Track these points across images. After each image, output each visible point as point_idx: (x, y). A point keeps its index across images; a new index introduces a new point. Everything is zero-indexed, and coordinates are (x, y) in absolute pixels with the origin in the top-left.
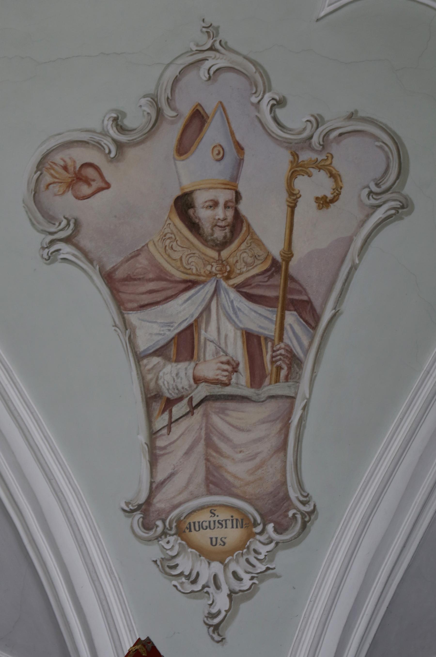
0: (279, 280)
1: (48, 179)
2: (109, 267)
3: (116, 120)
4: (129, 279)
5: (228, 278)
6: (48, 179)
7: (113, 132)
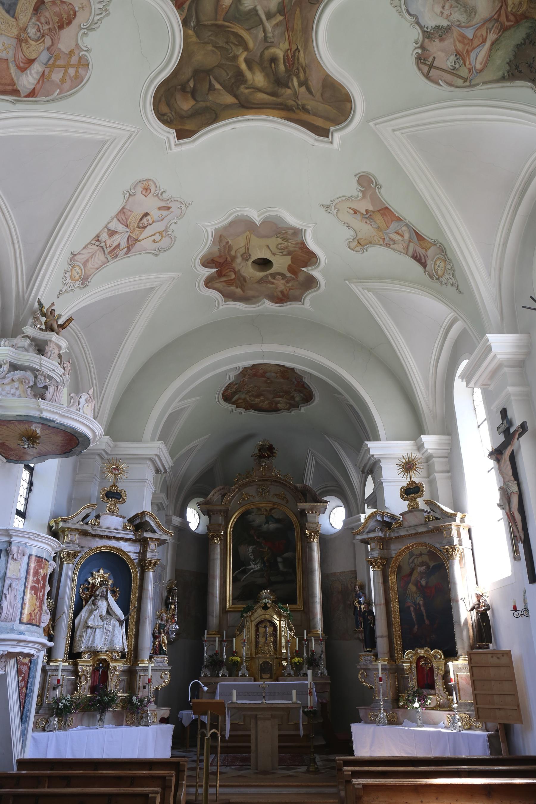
0: (134, 242)
1: (144, 183)
2: (126, 207)
3: (164, 191)
4: (124, 213)
5: (131, 232)
6: (144, 183)
7: (161, 192)
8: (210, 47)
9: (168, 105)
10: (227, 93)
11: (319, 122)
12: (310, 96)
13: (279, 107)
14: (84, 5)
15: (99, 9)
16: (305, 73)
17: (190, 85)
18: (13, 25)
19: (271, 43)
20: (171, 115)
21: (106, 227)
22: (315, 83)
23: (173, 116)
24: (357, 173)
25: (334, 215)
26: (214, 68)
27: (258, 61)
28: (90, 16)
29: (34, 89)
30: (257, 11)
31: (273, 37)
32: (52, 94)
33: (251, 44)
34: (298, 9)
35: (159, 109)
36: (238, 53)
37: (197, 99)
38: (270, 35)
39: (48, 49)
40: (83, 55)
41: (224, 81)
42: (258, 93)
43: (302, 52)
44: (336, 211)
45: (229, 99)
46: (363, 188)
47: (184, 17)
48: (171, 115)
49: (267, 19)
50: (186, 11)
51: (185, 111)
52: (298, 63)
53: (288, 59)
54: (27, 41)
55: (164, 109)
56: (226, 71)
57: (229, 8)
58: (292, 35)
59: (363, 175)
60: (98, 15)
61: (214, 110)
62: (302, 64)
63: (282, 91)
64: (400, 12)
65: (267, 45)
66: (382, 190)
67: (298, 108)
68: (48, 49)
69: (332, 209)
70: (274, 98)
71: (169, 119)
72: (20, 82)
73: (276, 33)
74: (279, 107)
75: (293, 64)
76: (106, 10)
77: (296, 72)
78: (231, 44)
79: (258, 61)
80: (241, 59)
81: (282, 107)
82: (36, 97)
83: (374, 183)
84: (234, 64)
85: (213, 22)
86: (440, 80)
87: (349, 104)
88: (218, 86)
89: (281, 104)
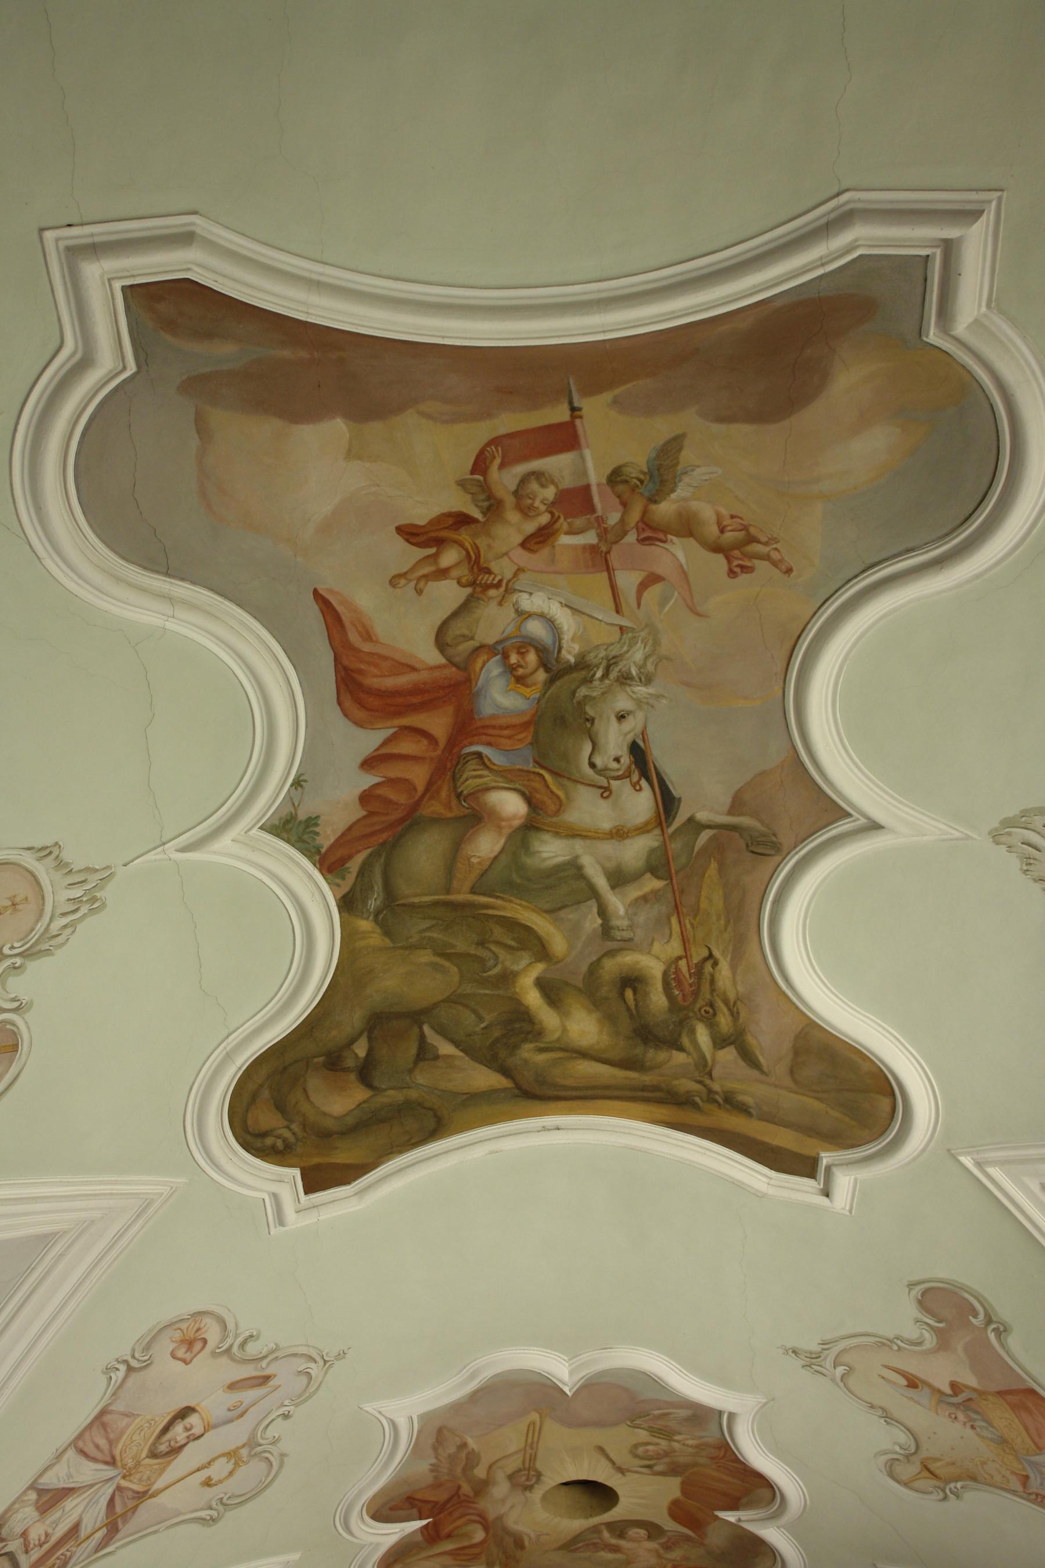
0: (131, 1504)
2: (112, 1408)
3: (251, 1336)
4: (104, 1426)
5: (124, 1477)
6: (184, 1326)
7: (240, 1339)
9: (280, 1107)
10: (477, 1065)
11: (784, 1139)
12: (755, 1073)
13: (649, 1095)
14: (18, 900)
15: (69, 900)
16: (735, 1015)
17: (357, 1051)
21: (32, 1487)
23: (294, 1134)
24: (916, 1278)
25: (833, 1380)
26: (435, 1005)
27: (581, 985)
28: (37, 921)
30: (580, 868)
31: (631, 927)
33: (558, 944)
34: (714, 865)
35: (250, 1122)
36: (515, 968)
37: (376, 1083)
42: (581, 1061)
44: (840, 1370)
45: (484, 1078)
47: (345, 888)
48: (287, 1134)
49: (613, 887)
50: (351, 878)
51: (335, 1118)
53: (679, 981)
55: (266, 1118)
56: (475, 1012)
57: (491, 864)
58: (692, 925)
59: (938, 1288)
60: (64, 914)
61: (430, 1109)
62: (725, 992)
63: (656, 1056)
65: (610, 945)
66: (1013, 1341)
69: (829, 1363)
71: (280, 1144)
73: (641, 918)
74: (649, 1095)
75: (696, 994)
76: (94, 899)
78: (493, 948)
79: (581, 985)
81: (658, 1094)
84: (501, 992)
85: (436, 897)
88: (446, 1048)
89: (656, 1088)
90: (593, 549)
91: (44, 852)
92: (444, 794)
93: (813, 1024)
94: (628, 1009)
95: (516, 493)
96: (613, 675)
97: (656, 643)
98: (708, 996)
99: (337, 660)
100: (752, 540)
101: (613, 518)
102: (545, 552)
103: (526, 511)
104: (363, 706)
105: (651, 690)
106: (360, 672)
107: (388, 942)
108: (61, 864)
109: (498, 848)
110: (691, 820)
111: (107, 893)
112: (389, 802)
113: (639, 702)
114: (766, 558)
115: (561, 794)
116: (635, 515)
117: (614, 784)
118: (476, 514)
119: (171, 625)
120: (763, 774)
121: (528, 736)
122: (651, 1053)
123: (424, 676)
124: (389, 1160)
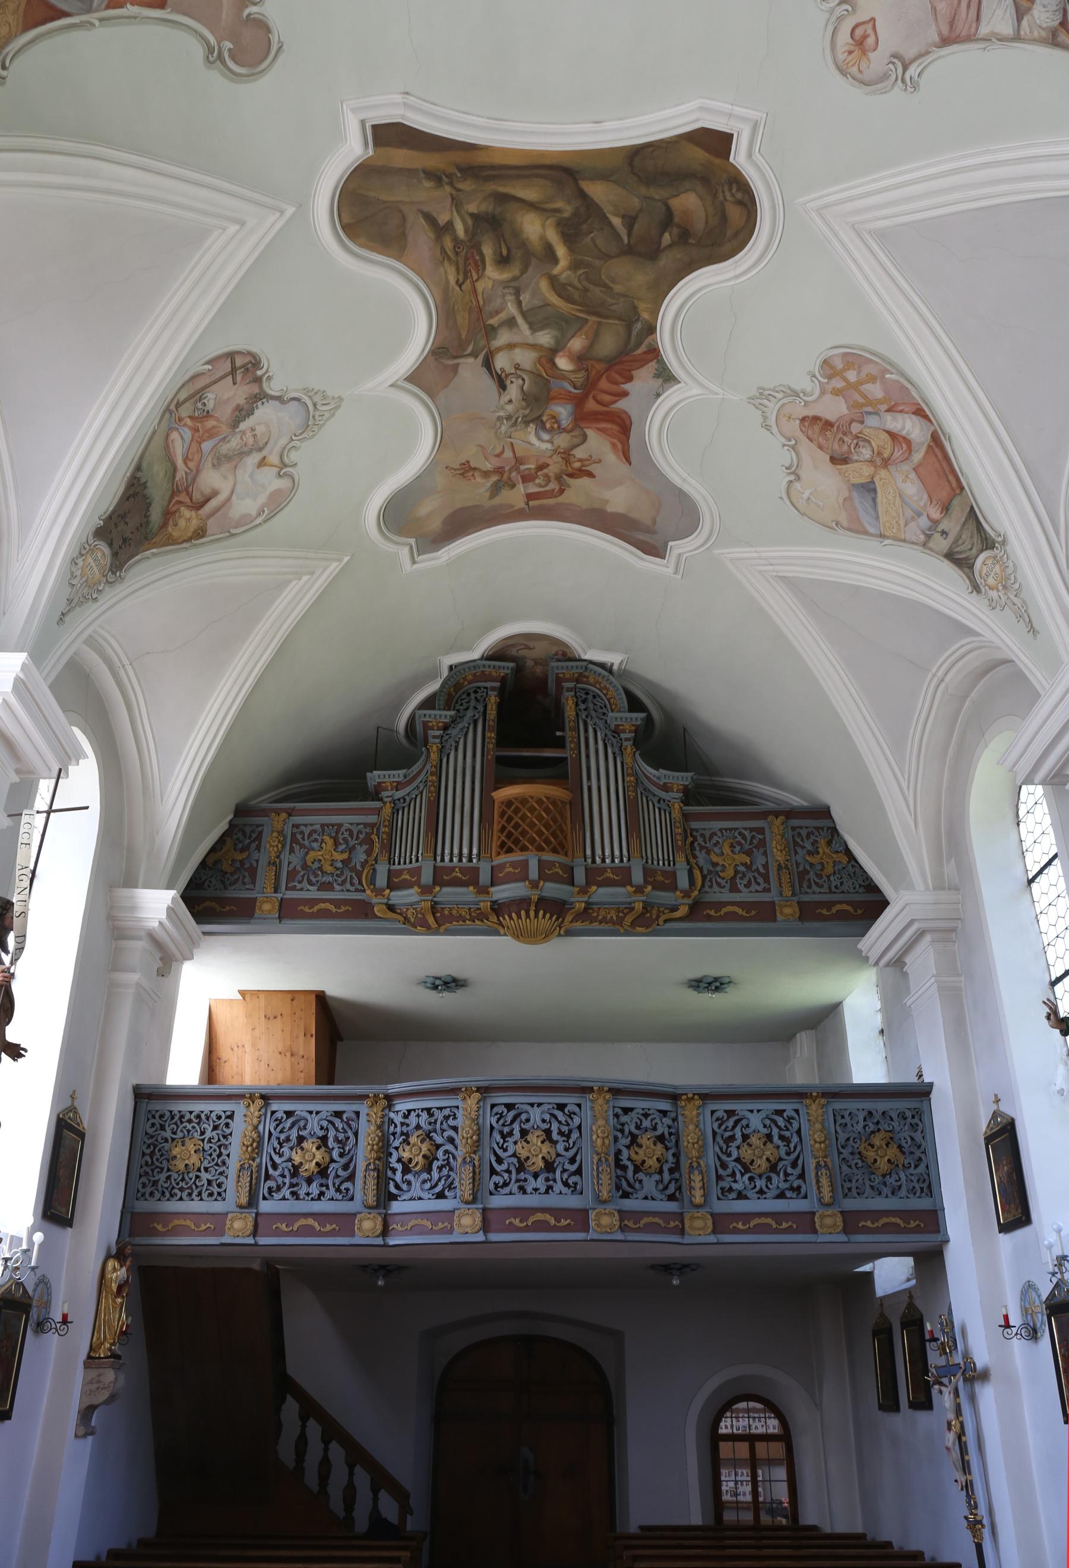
1: (854, 70)
2: (937, 39)
4: (952, 24)
6: (854, 70)
8: (618, 288)
9: (724, 218)
11: (401, 157)
12: (426, 209)
16: (443, 250)
17: (669, 237)
18: (881, 479)
19: (508, 287)
20: (728, 194)
21: (1017, 38)
22: (421, 238)
23: (723, 192)
24: (282, 58)
26: (617, 256)
29: (914, 413)
31: (504, 296)
32: (898, 381)
33: (544, 285)
34: (463, 337)
35: (744, 219)
36: (569, 272)
37: (664, 208)
38: (510, 298)
39: (862, 422)
40: (824, 378)
41: (602, 229)
43: (452, 280)
45: (597, 191)
46: (249, 15)
47: (651, 337)
48: (728, 194)
49: (514, 318)
50: (646, 342)
51: (696, 192)
52: (457, 264)
53: (476, 266)
54: (879, 454)
55: (735, 214)
56: (596, 246)
60: (775, 397)
61: (634, 174)
63: (487, 207)
64: (307, 391)
65: (515, 284)
66: (198, 51)
67: (450, 176)
68: (862, 422)
70: (502, 189)
71: (734, 191)
72: (922, 439)
75: (466, 259)
76: (761, 394)
77: (459, 248)
78: (580, 287)
80: (563, 263)
82: (919, 404)
83: (226, 55)
84: (579, 257)
86: (211, 368)
87: (346, 221)
88: (616, 221)
90: (522, 464)
91: (768, 427)
92: (594, 372)
93: (399, 258)
94: (505, 241)
95: (550, 482)
96: (514, 419)
97: (496, 433)
98: (459, 259)
99: (628, 439)
100: (462, 474)
101: (514, 474)
102: (540, 463)
103: (547, 476)
104: (622, 419)
105: (497, 414)
106: (619, 432)
107: (636, 302)
108: (765, 418)
109: (571, 342)
110: (476, 357)
111: (754, 392)
112: (620, 374)
113: (502, 408)
114: (455, 470)
115: (539, 366)
116: (505, 476)
117: (513, 371)
118: (565, 477)
119: (685, 475)
120: (446, 387)
121: (553, 394)
122: (490, 209)
123: (594, 426)
124: (671, 138)
